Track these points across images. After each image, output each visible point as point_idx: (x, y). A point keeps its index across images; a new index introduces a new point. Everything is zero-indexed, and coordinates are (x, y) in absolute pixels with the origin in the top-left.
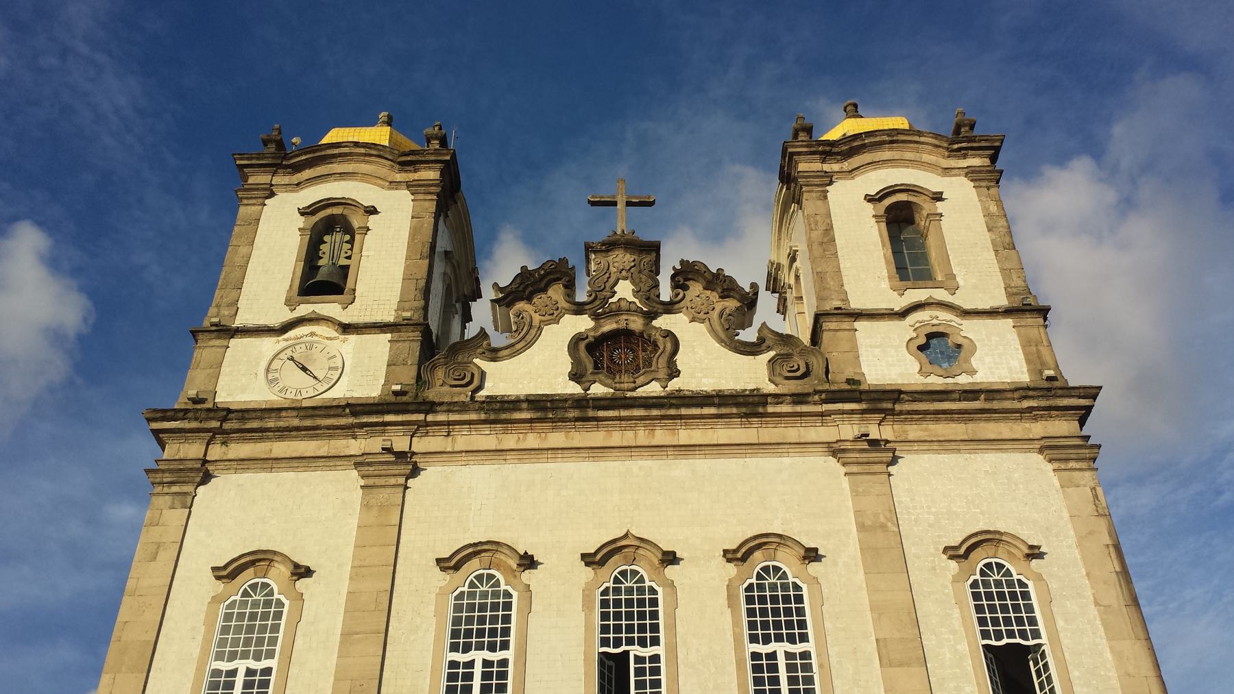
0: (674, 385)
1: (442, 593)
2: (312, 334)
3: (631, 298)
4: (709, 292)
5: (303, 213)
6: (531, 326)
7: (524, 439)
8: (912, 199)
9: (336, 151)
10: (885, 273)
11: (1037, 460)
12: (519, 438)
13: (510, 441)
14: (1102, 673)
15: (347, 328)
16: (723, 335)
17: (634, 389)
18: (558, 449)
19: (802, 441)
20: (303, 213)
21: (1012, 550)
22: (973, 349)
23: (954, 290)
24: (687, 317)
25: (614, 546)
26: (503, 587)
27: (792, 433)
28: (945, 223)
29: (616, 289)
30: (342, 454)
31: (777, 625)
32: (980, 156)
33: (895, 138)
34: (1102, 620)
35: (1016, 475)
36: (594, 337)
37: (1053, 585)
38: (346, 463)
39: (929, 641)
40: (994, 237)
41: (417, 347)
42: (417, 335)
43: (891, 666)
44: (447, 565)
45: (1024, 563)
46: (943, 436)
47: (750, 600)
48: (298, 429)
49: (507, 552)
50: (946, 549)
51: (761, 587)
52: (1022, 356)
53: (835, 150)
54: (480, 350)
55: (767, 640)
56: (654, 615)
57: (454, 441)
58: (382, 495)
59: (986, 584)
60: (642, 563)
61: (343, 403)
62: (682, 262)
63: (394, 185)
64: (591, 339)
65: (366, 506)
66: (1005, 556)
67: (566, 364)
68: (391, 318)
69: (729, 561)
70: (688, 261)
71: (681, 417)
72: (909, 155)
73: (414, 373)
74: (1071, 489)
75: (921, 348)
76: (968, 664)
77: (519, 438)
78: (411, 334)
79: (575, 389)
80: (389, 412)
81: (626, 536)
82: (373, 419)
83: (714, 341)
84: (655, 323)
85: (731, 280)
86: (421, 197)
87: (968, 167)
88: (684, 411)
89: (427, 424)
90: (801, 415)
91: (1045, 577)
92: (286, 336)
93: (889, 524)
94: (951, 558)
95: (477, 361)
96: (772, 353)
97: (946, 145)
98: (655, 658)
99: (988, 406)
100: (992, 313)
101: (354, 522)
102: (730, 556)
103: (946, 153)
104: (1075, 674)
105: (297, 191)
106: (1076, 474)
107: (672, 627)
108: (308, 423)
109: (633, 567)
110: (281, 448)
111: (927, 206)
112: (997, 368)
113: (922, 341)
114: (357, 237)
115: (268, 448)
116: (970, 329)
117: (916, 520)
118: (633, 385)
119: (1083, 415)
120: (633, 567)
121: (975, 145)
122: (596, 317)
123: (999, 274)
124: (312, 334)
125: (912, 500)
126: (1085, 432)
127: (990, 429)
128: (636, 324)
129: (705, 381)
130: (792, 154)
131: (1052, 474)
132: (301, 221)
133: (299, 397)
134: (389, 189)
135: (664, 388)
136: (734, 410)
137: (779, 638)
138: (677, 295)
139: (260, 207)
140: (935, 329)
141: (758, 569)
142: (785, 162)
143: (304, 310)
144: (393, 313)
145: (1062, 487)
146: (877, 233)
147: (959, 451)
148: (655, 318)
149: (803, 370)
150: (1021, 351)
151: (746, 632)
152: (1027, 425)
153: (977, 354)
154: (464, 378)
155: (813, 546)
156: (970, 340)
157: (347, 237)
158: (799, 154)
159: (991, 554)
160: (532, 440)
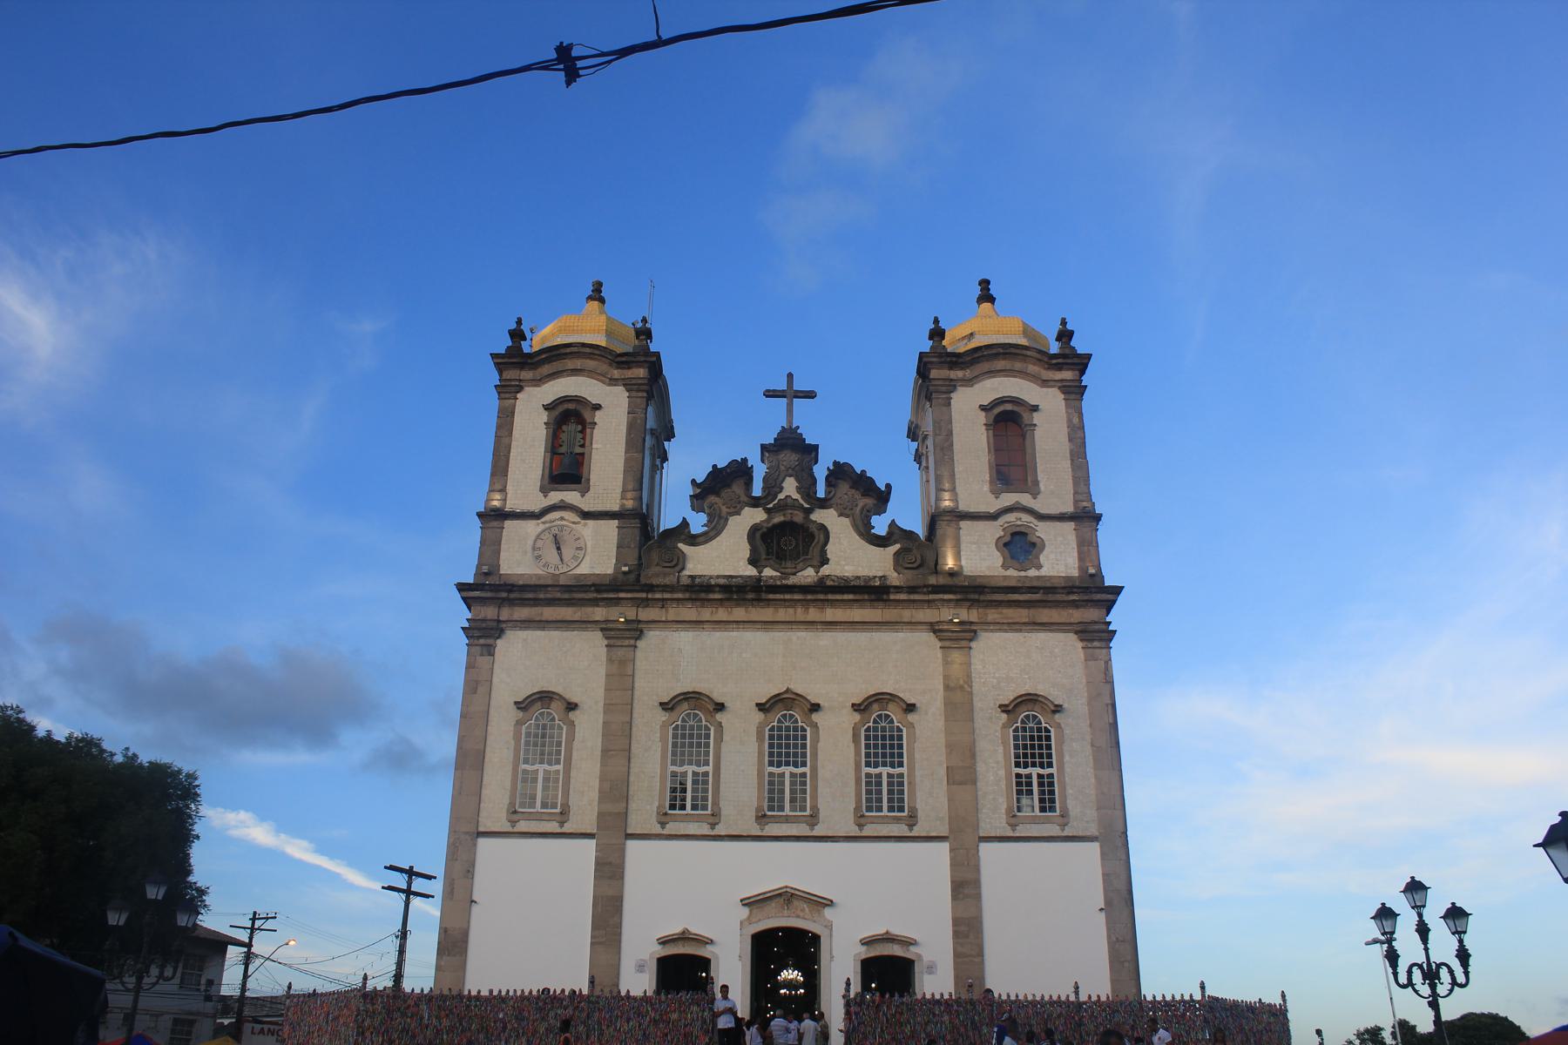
0: (825, 570)
1: (664, 726)
2: (562, 519)
3: (796, 496)
4: (854, 491)
5: (547, 408)
6: (720, 517)
7: (716, 612)
8: (1016, 408)
9: (568, 350)
10: (987, 477)
11: (1071, 638)
13: (706, 614)
14: (1087, 792)
15: (587, 515)
17: (794, 574)
18: (740, 622)
19: (913, 620)
20: (547, 408)
21: (1046, 707)
22: (1043, 547)
23: (1035, 496)
24: (837, 511)
25: (777, 698)
26: (704, 723)
27: (907, 614)
28: (1038, 433)
29: (784, 485)
30: (591, 619)
31: (884, 755)
32: (1073, 370)
33: (1008, 351)
34: (1093, 756)
35: (1056, 650)
36: (767, 528)
37: (1067, 731)
38: (594, 626)
39: (981, 768)
40: (1072, 447)
41: (637, 532)
42: (636, 523)
43: (953, 784)
44: (667, 707)
45: (1050, 715)
46: (1011, 618)
47: (867, 738)
48: (559, 599)
49: (707, 700)
50: (1000, 706)
51: (875, 729)
52: (1076, 554)
53: (961, 360)
54: (683, 537)
55: (876, 766)
56: (804, 747)
57: (667, 612)
58: (620, 653)
59: (1024, 729)
61: (589, 583)
62: (835, 463)
63: (613, 382)
64: (765, 530)
65: (610, 660)
67: (746, 551)
68: (616, 508)
69: (855, 710)
70: (839, 462)
71: (828, 600)
72: (1018, 365)
73: (636, 555)
74: (1090, 663)
75: (1006, 545)
76: (1003, 784)
78: (633, 521)
79: (751, 571)
80: (622, 591)
81: (788, 691)
82: (612, 595)
83: (855, 534)
84: (814, 517)
85: (871, 481)
86: (634, 394)
87: (1062, 380)
88: (830, 597)
89: (647, 599)
90: (914, 601)
91: (1063, 726)
92: (543, 520)
93: (966, 686)
94: (1003, 711)
95: (681, 545)
96: (898, 546)
97: (1046, 359)
98: (804, 775)
99: (1045, 598)
100: (1061, 518)
101: (600, 672)
102: (856, 707)
103: (1046, 366)
104: (1069, 791)
105: (539, 386)
106: (1098, 651)
108: (566, 596)
110: (549, 613)
111: (1025, 416)
112: (1057, 564)
113: (1007, 539)
114: (588, 431)
115: (540, 611)
116: (1043, 530)
117: (984, 683)
118: (794, 570)
119: (1110, 606)
120: (791, 712)
121: (1069, 361)
122: (768, 511)
123: (1071, 481)
124: (562, 519)
125: (984, 667)
126: (1108, 619)
127: (1046, 615)
128: (798, 518)
129: (846, 568)
130: (926, 363)
131: (1081, 650)
132: (544, 416)
133: (557, 572)
134: (610, 385)
135: (817, 573)
136: (866, 597)
137: (884, 765)
138: (830, 492)
139: (513, 401)
140: (1018, 529)
141: (874, 716)
143: (555, 497)
144: (618, 501)
145: (1086, 660)
146: (986, 439)
147: (1021, 631)
148: (811, 513)
149: (919, 562)
150: (1076, 550)
151: (863, 760)
152: (1071, 611)
153: (1045, 552)
154: (672, 561)
155: (912, 701)
156: (1043, 540)
157: (580, 427)
158: (932, 363)
159: (1030, 709)
160: (722, 614)
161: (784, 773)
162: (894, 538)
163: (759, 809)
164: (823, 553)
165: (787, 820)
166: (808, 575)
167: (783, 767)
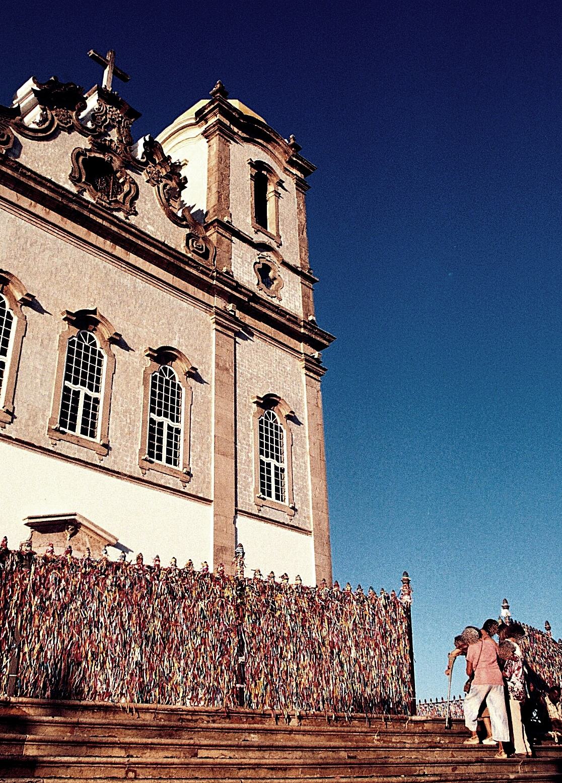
0: (133, 220)
12: (31, 203)
16: (164, 200)
54: (13, 121)
60: (97, 333)
66: (277, 411)
75: (259, 269)
77: (31, 203)
81: (94, 312)
100: (294, 269)
107: (110, 384)
109: (91, 334)
120: (91, 334)
122: (94, 143)
129: (149, 226)
142: (209, 106)
161: (79, 391)
162: (184, 223)
163: (51, 421)
164: (132, 203)
165: (78, 442)
166: (121, 215)
167: (79, 386)
